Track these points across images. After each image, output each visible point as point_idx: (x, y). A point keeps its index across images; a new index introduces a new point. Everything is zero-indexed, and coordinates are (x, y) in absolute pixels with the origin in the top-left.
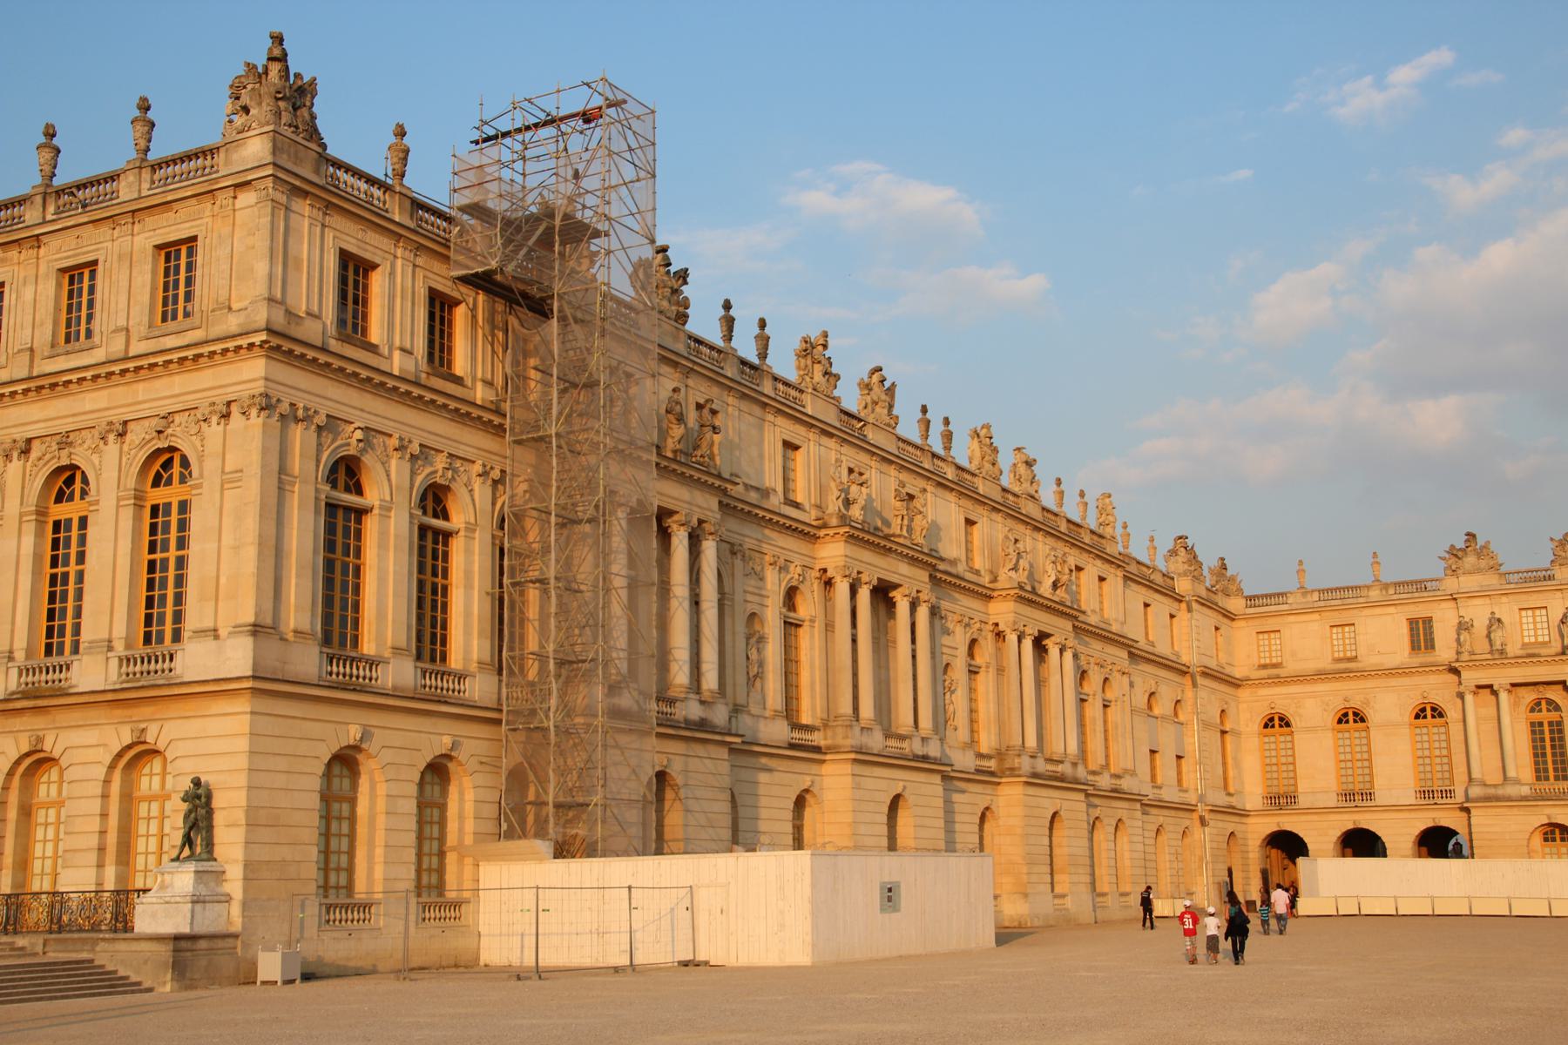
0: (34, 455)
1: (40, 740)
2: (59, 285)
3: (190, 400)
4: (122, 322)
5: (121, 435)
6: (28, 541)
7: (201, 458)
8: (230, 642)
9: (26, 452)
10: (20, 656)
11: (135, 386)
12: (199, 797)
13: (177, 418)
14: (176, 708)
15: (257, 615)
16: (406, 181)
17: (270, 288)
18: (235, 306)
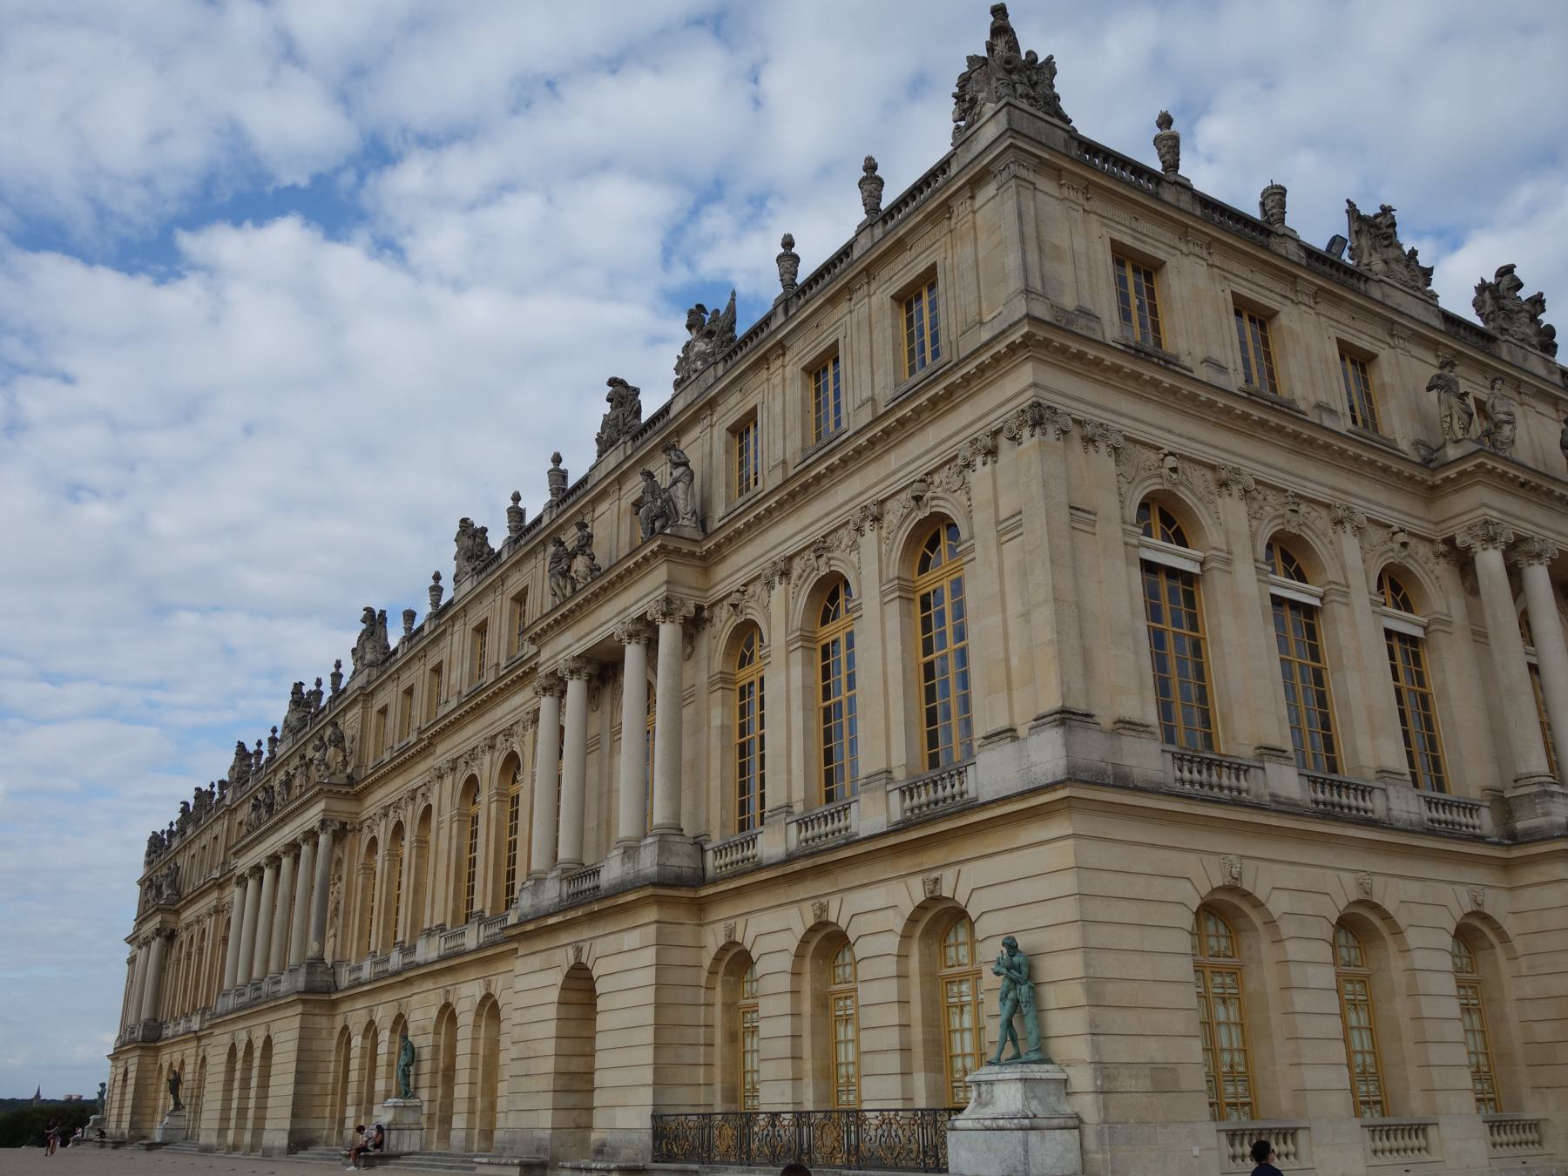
0: (795, 575)
1: (824, 909)
2: (805, 386)
3: (947, 450)
4: (866, 394)
5: (877, 519)
6: (797, 672)
7: (969, 514)
8: (1034, 740)
9: (785, 574)
10: (798, 808)
11: (886, 458)
12: (1018, 968)
13: (936, 478)
14: (971, 848)
15: (1063, 697)
16: (1180, 172)
17: (1026, 279)
18: (986, 318)
